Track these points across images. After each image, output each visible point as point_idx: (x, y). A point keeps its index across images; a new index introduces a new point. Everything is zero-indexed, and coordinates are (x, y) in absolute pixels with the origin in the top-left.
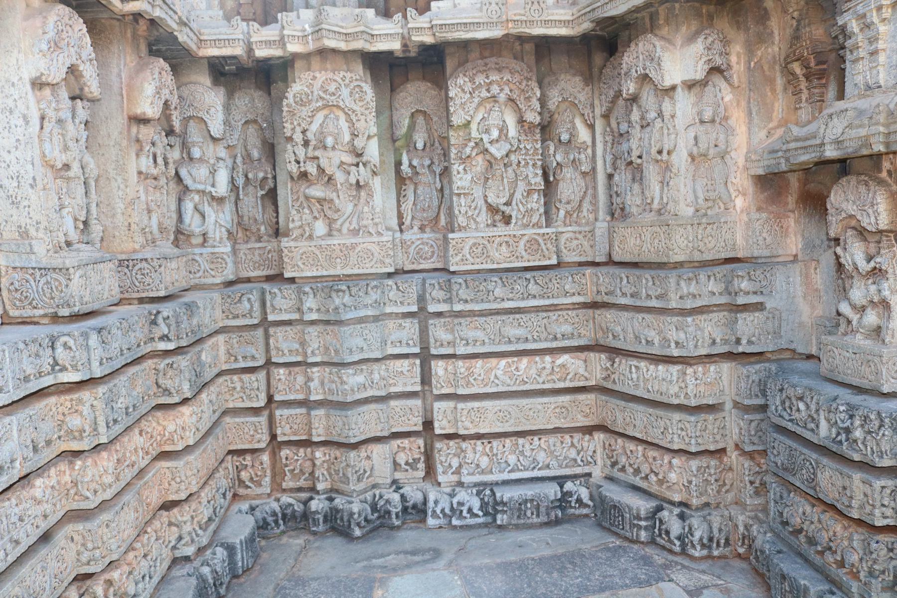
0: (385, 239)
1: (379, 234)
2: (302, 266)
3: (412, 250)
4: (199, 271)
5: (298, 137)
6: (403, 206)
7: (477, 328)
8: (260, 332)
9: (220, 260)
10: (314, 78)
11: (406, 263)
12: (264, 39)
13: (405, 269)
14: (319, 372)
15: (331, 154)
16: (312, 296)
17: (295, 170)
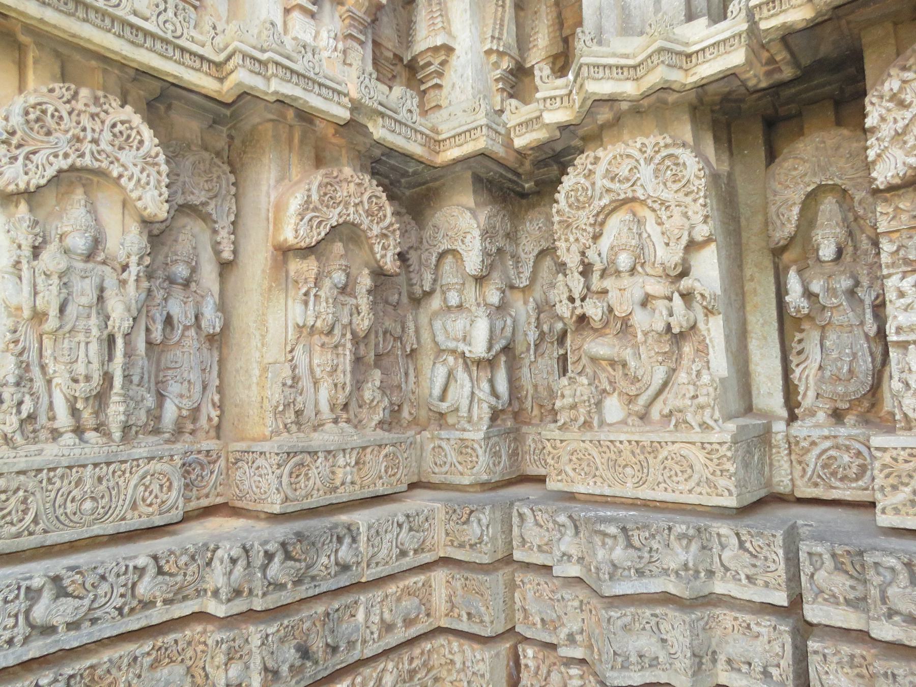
0: (715, 437)
1: (705, 426)
2: (571, 473)
3: (811, 457)
4: (445, 463)
5: (572, 260)
6: (798, 371)
8: (501, 576)
9: (469, 450)
10: (597, 160)
11: (799, 482)
13: (798, 495)
14: (582, 677)
15: (626, 281)
16: (570, 532)
17: (567, 314)
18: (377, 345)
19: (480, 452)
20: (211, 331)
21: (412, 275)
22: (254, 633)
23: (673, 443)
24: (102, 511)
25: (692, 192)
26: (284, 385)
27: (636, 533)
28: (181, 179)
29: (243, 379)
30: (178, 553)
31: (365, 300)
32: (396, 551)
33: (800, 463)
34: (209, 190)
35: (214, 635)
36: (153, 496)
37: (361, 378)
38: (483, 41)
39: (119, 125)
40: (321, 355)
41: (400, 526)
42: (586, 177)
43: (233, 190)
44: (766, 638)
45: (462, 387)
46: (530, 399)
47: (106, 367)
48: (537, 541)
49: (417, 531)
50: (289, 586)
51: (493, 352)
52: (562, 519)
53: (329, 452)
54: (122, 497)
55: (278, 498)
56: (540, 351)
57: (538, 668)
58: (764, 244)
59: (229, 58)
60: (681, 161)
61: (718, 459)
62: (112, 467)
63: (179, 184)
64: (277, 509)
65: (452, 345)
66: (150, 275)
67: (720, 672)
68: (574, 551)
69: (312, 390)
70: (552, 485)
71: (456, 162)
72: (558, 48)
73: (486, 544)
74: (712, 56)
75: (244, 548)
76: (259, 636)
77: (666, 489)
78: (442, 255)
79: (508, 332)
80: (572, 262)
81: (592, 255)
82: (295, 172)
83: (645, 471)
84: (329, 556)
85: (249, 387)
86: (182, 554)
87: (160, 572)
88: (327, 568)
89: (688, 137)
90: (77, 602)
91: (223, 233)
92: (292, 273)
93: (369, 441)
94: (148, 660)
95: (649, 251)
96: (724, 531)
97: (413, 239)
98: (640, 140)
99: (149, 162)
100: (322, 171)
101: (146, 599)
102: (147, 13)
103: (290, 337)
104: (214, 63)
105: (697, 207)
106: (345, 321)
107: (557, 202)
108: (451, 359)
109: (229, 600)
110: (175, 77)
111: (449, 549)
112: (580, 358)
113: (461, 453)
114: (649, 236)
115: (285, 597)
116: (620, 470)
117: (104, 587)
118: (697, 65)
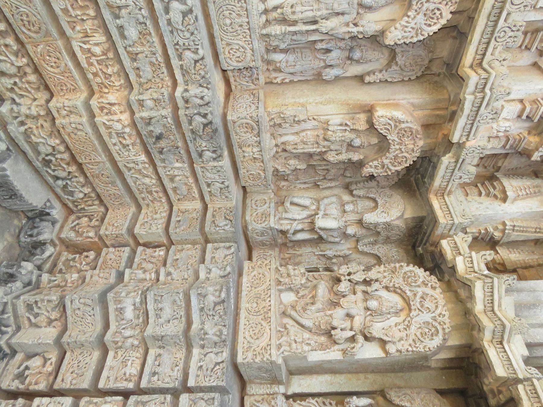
0: (274, 352)
1: (279, 346)
2: (253, 274)
4: (257, 206)
5: (373, 274)
6: (314, 401)
8: (199, 237)
9: (264, 219)
10: (434, 288)
11: (252, 398)
12: (459, 245)
13: (246, 398)
14: (151, 279)
15: (361, 305)
16: (222, 273)
17: (341, 272)
18: (320, 165)
19: (263, 225)
20: (323, 74)
21: (362, 184)
22: (167, 112)
23: (270, 329)
24: (225, 29)
25: (416, 344)
26: (295, 116)
27: (222, 308)
28: (411, 49)
29: (298, 94)
30: (205, 69)
31: (345, 158)
32: (209, 181)
33: (263, 399)
34: (405, 66)
35: (166, 92)
36: (234, 53)
37: (301, 158)
38: (512, 220)
39: (439, 12)
40: (313, 135)
41: (223, 183)
42: (423, 282)
43: (406, 79)
44: (171, 374)
45: (299, 214)
46: (294, 252)
47: (300, 21)
48: (217, 256)
49: (220, 192)
50: (191, 127)
51: (318, 231)
52: (229, 269)
53: (260, 143)
54: (233, 38)
55: (235, 118)
56: (321, 258)
57: (155, 257)
58: (387, 386)
59: (485, 70)
60: (434, 337)
61: (262, 353)
62: (247, 31)
63: (408, 49)
64: (229, 118)
65: (322, 207)
66: (353, 38)
67: (155, 350)
68: (212, 275)
69: (293, 132)
70: (247, 264)
71: (431, 206)
72: (509, 266)
73: (215, 229)
74: (501, 357)
75: (209, 103)
76: (166, 114)
77: (245, 325)
78: (374, 200)
79: (332, 239)
80: (371, 275)
81: (375, 286)
82: (419, 113)
83: (255, 314)
84: (206, 147)
85: (294, 98)
86: (205, 71)
87: (196, 62)
88: (200, 146)
89: (450, 343)
90: (180, 23)
91: (380, 76)
92: (358, 116)
93: (267, 164)
94: (154, 60)
95: (379, 318)
96: (224, 354)
97: (383, 183)
98: (447, 314)
99: (418, 31)
100: (419, 129)
101: (183, 56)
102: (510, 21)
103: (322, 117)
104: (482, 62)
105: (406, 346)
106: (332, 147)
107: (408, 266)
108: (314, 207)
109: (183, 97)
110: (471, 41)
111: (212, 209)
112: (316, 279)
113: (262, 215)
114: (388, 319)
115: (185, 125)
116: (255, 301)
117: (187, 35)
118: (496, 348)
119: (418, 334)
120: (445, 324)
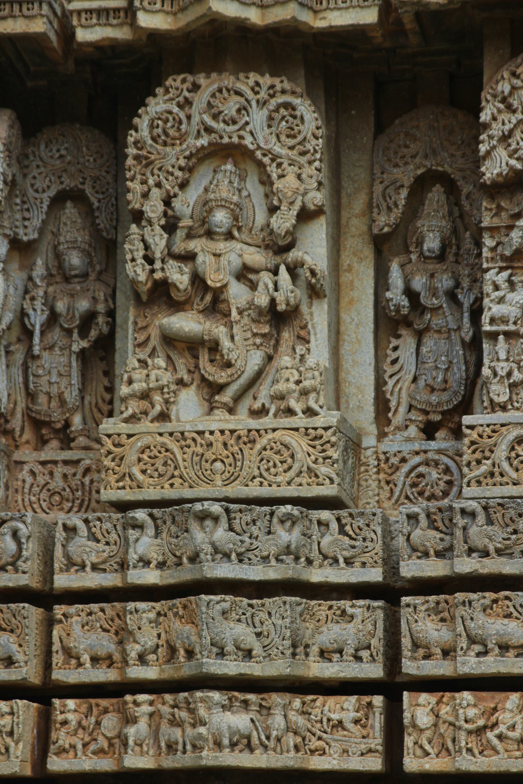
0: (319, 421)
1: (310, 412)
2: (140, 477)
3: (400, 477)
5: (154, 208)
6: (391, 383)
7: (509, 616)
10: (195, 88)
14: (151, 703)
15: (221, 246)
17: (142, 277)
23: (274, 430)
25: (308, 152)
33: (388, 483)
42: (179, 105)
44: (360, 618)
46: (19, 415)
58: (365, 228)
60: (298, 113)
61: (322, 445)
67: (312, 664)
74: (344, 5)
77: (261, 484)
80: (153, 211)
83: (239, 464)
98: (253, 77)
114: (249, 195)
116: (208, 466)
118: (328, 8)
119: (291, 142)
120: (272, 87)
